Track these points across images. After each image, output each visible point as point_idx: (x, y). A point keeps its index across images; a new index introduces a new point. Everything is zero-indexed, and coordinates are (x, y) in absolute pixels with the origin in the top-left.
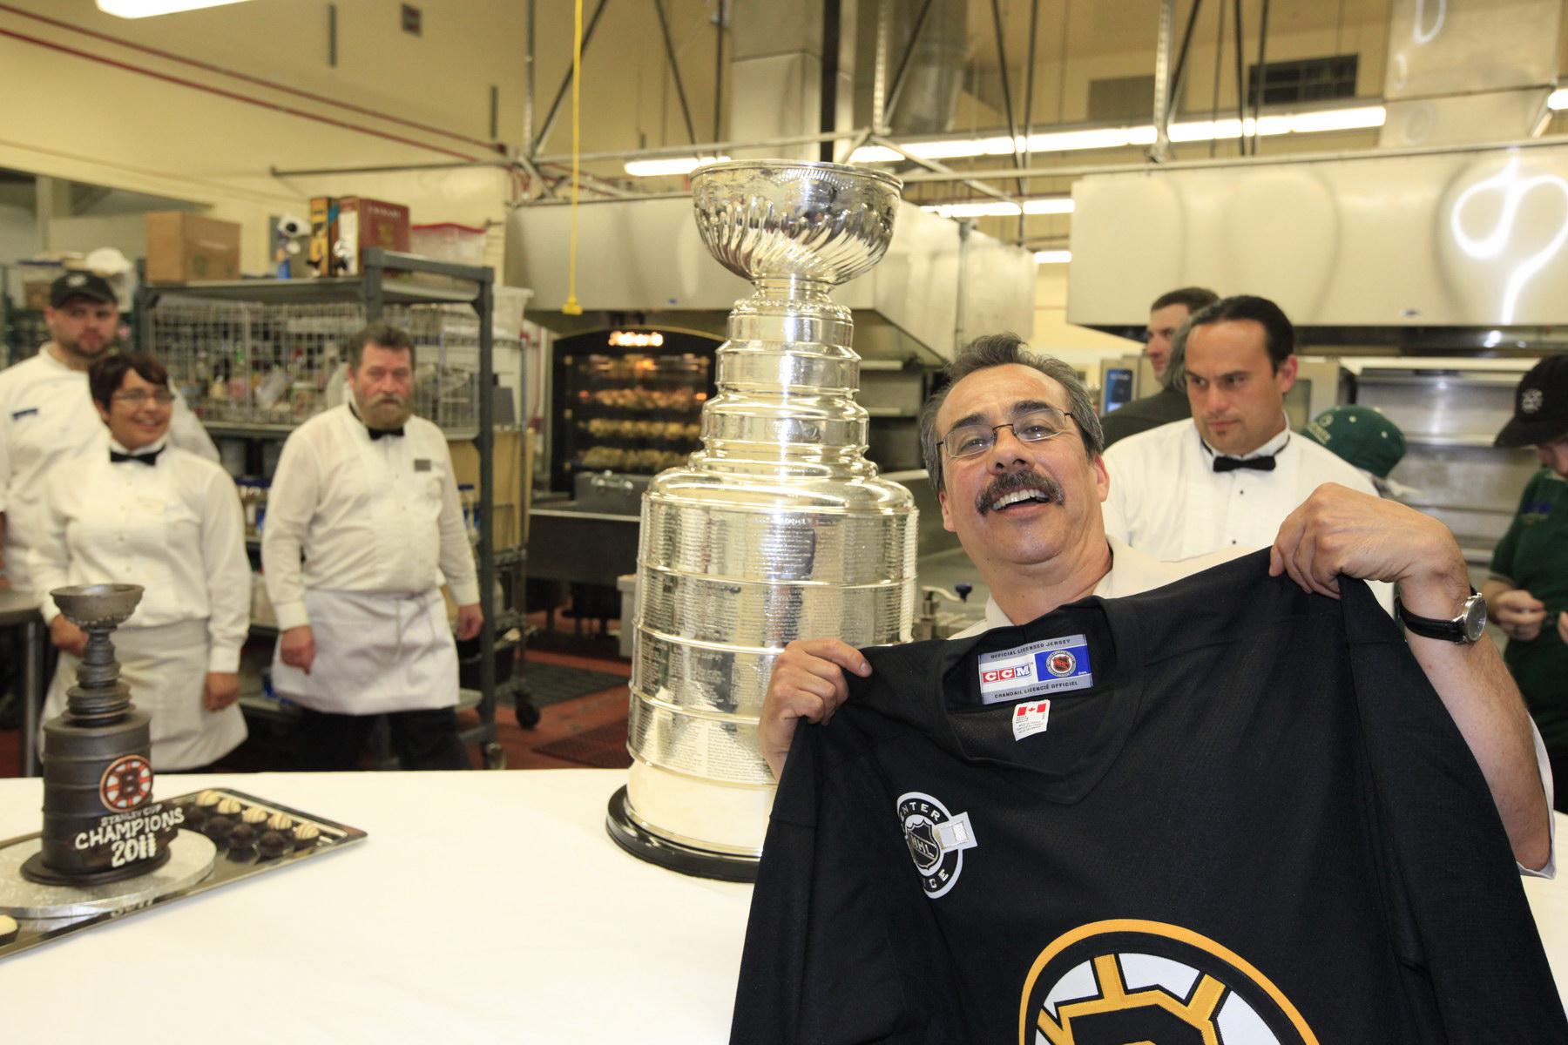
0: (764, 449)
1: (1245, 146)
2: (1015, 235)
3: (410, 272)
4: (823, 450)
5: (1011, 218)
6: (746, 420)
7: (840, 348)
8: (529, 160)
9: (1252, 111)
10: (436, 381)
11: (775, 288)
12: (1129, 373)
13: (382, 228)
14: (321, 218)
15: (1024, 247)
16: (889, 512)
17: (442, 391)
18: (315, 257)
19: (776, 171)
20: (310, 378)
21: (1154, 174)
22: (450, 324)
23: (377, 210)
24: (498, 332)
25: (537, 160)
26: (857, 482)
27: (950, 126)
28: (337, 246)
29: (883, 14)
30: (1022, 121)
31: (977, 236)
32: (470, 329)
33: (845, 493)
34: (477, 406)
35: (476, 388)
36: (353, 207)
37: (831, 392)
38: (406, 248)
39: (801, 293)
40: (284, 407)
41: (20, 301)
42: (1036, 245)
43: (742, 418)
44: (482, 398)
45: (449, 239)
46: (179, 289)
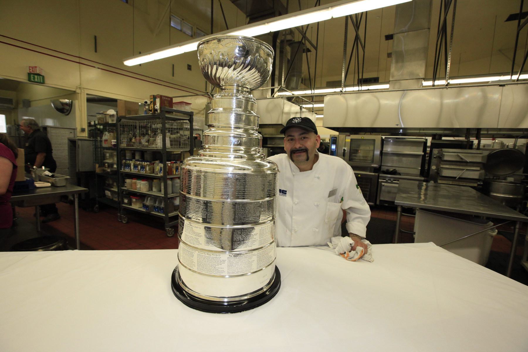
0: (223, 148)
1: (359, 92)
2: (312, 110)
3: (173, 112)
4: (244, 149)
5: (311, 108)
6: (216, 137)
7: (252, 112)
8: (211, 95)
9: (361, 85)
10: (180, 138)
11: (228, 89)
12: (336, 138)
13: (166, 102)
14: (152, 100)
15: (314, 112)
16: (269, 172)
17: (182, 140)
18: (151, 109)
19: (222, 39)
20: (153, 137)
21: (342, 95)
22: (185, 125)
23: (164, 98)
24: (194, 127)
25: (212, 94)
26: (258, 161)
27: (299, 88)
28: (155, 106)
29: (284, 62)
30: (313, 87)
31: (303, 110)
32: (189, 127)
33: (249, 165)
34: (190, 143)
35: (190, 139)
36: (159, 98)
37: (248, 127)
38: (172, 108)
39: (238, 91)
40: (147, 144)
41: (97, 122)
42: (316, 112)
43: (215, 136)
44: (191, 142)
45: (182, 105)
46: (124, 117)
